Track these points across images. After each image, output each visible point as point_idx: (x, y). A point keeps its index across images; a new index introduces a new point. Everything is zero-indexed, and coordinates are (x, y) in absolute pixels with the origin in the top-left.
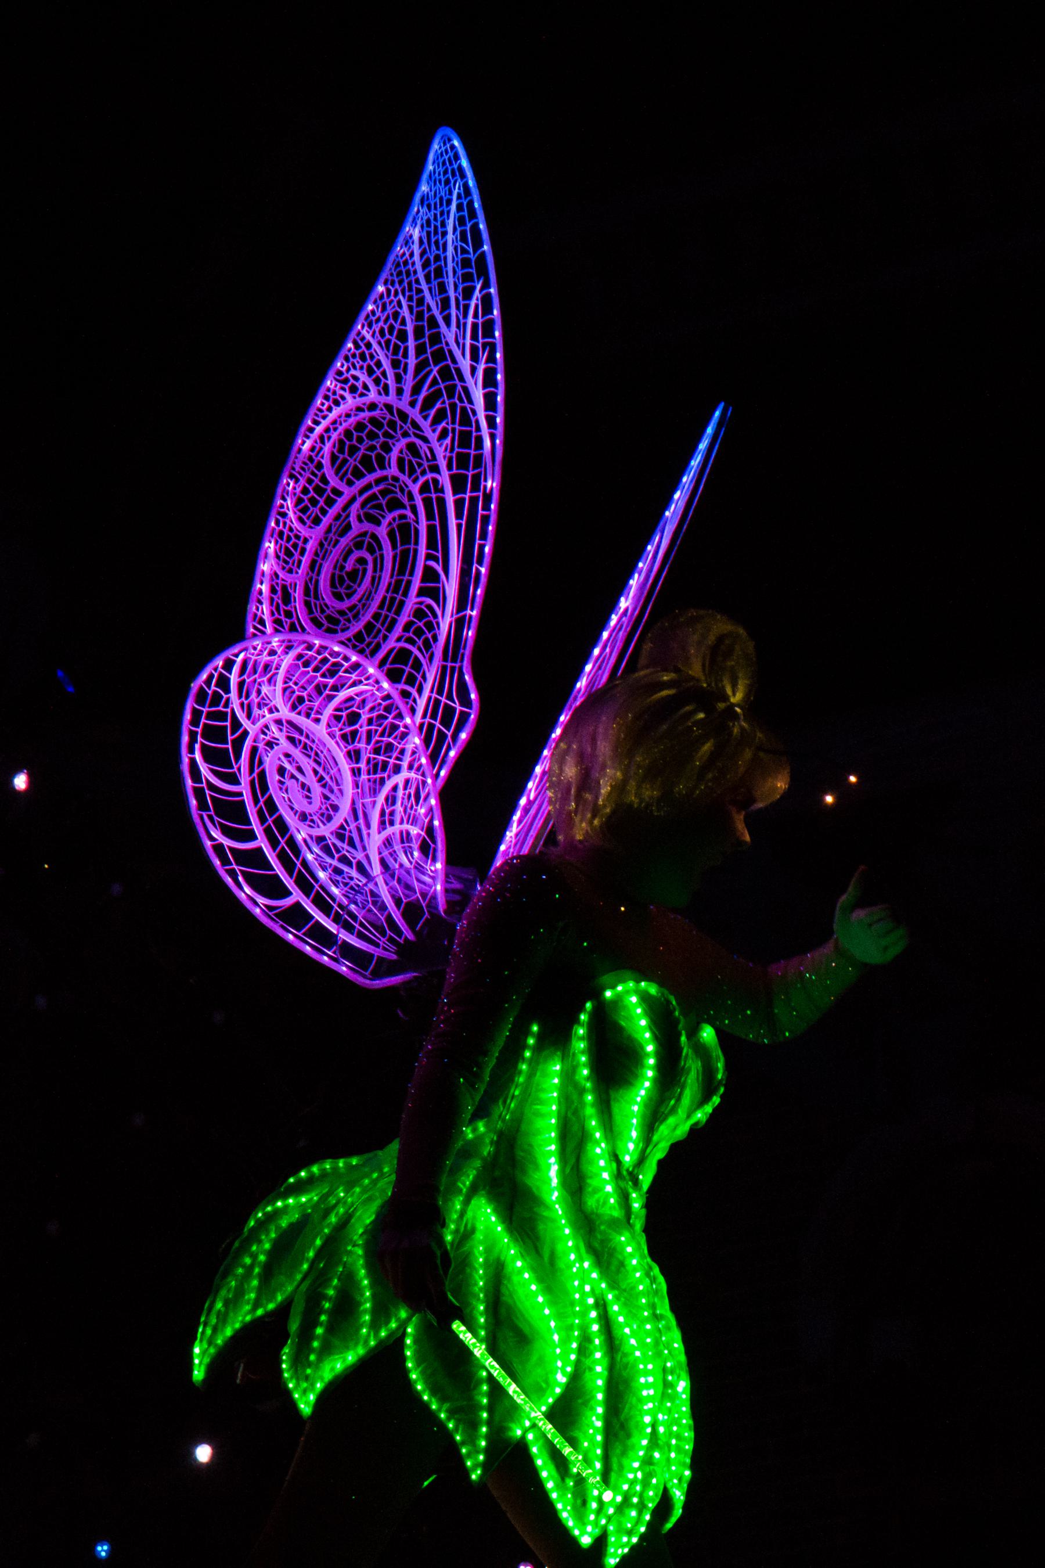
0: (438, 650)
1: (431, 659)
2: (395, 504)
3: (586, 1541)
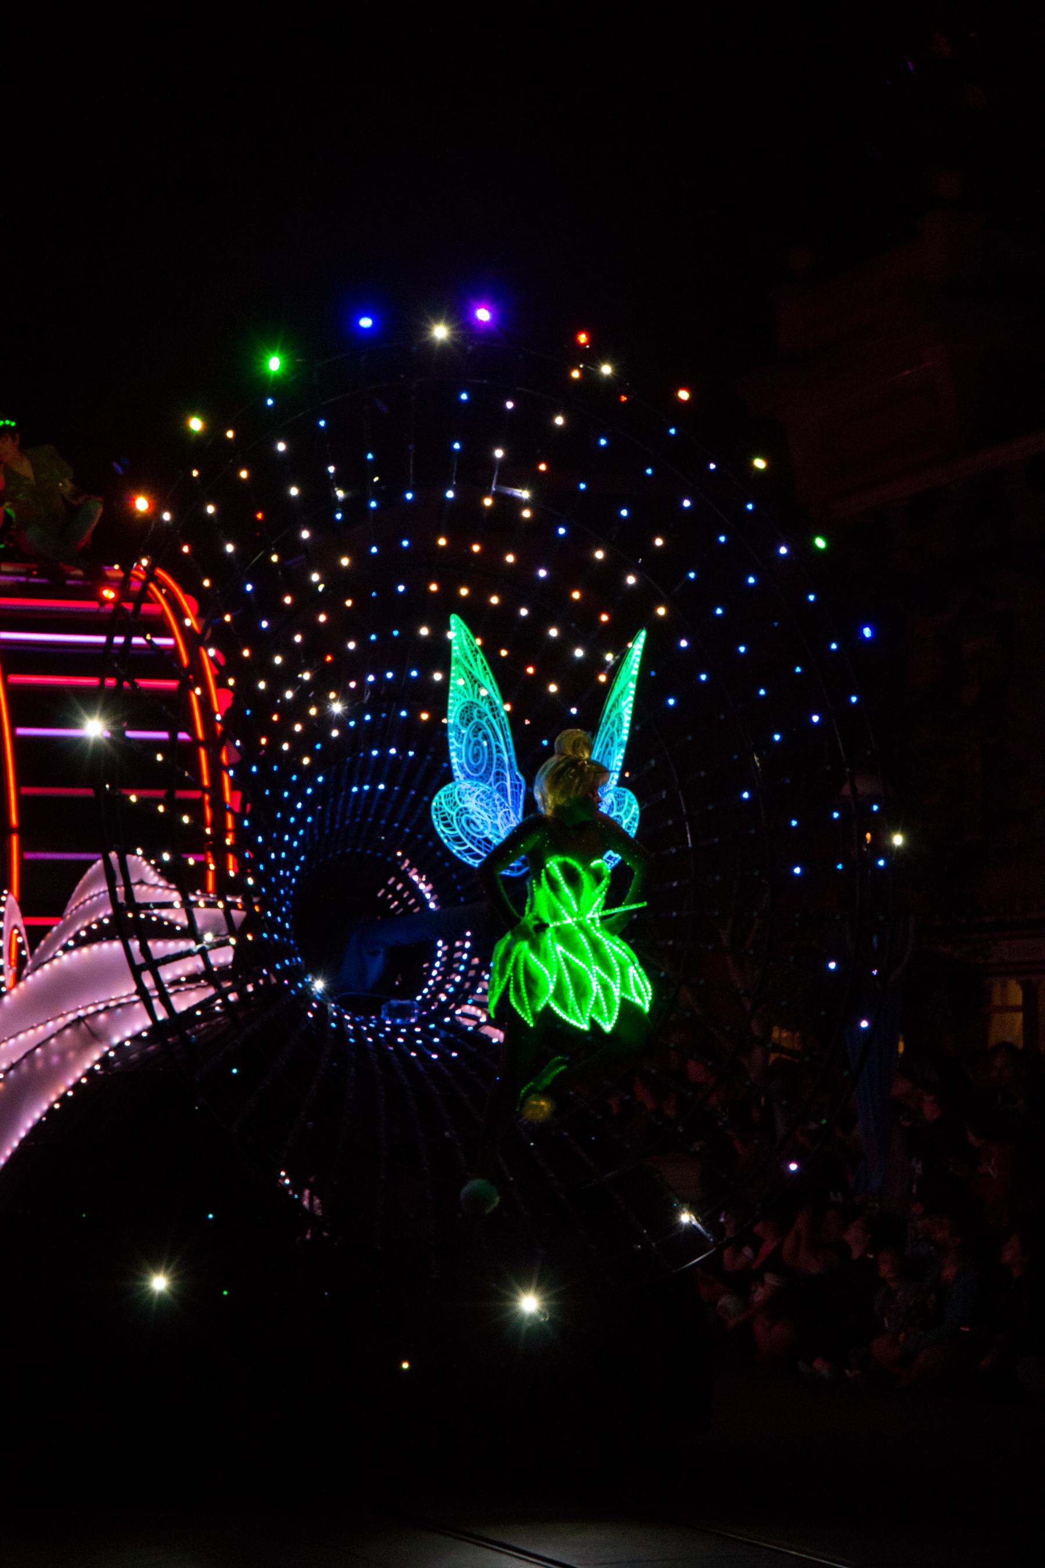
0: (507, 769)
1: (505, 771)
2: (480, 730)
3: (585, 1027)
